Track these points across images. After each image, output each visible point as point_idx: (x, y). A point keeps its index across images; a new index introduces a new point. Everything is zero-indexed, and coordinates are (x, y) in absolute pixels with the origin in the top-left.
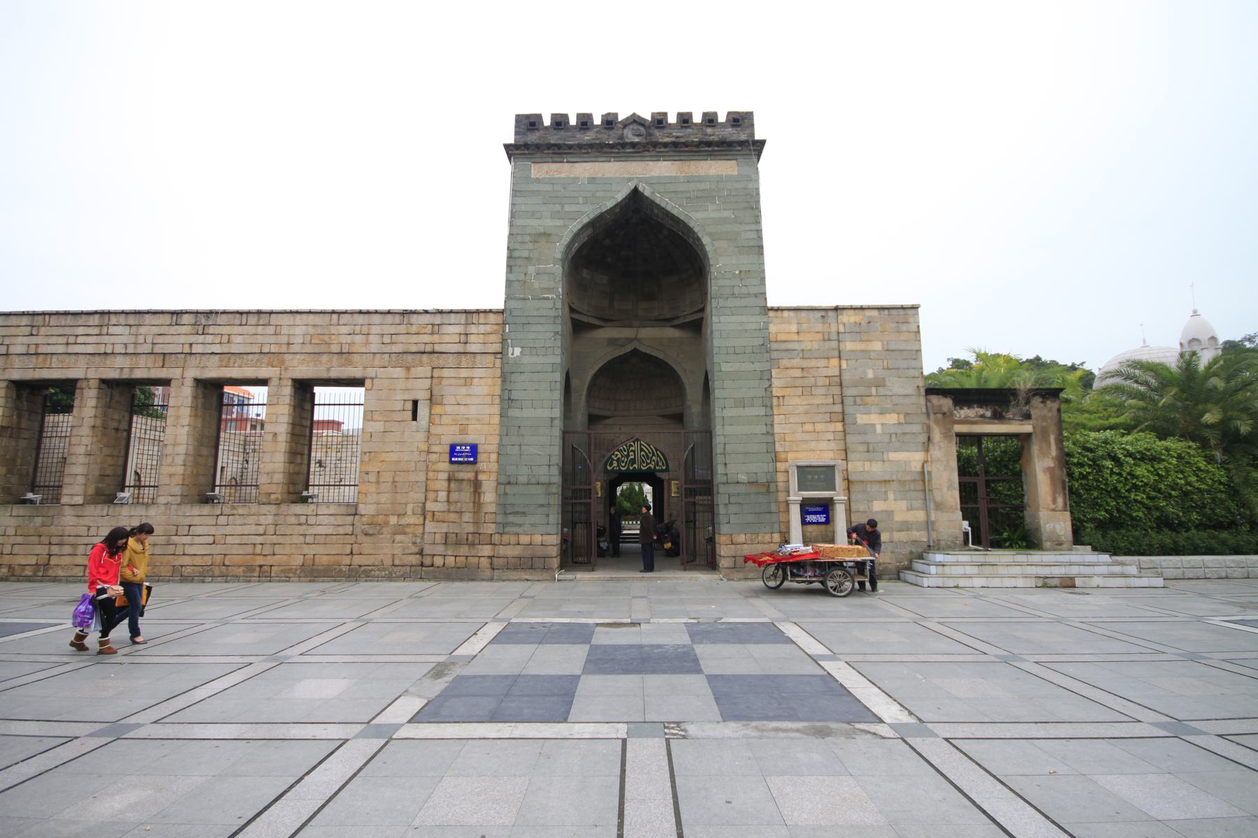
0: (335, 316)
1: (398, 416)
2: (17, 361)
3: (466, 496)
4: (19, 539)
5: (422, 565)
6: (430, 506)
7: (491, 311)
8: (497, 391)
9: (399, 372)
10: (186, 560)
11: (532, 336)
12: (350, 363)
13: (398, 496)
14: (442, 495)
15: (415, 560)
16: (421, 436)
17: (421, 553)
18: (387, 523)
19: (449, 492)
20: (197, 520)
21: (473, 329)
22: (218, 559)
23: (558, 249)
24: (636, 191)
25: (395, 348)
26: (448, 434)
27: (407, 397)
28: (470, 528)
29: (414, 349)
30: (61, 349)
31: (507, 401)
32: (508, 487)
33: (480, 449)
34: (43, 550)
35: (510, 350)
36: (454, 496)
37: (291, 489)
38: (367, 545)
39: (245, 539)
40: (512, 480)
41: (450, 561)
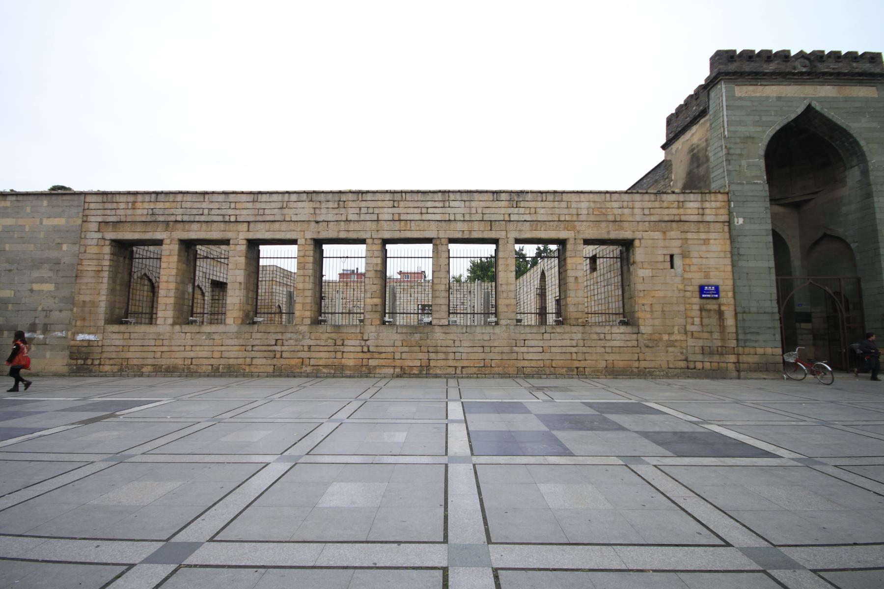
0: (608, 195)
1: (661, 266)
3: (714, 321)
4: (406, 349)
5: (688, 368)
6: (689, 328)
8: (728, 248)
9: (658, 235)
10: (526, 364)
11: (750, 210)
12: (622, 228)
13: (667, 321)
14: (697, 320)
15: (683, 364)
16: (678, 280)
17: (686, 360)
18: (661, 339)
19: (701, 318)
20: (529, 336)
21: (707, 205)
22: (548, 363)
23: (761, 147)
24: (809, 108)
25: (653, 218)
26: (698, 279)
27: (666, 252)
28: (719, 343)
29: (666, 218)
31: (735, 256)
32: (745, 316)
33: (721, 289)
34: (424, 356)
35: (736, 220)
36: (706, 321)
38: (648, 354)
39: (564, 349)
40: (747, 310)
41: (707, 365)
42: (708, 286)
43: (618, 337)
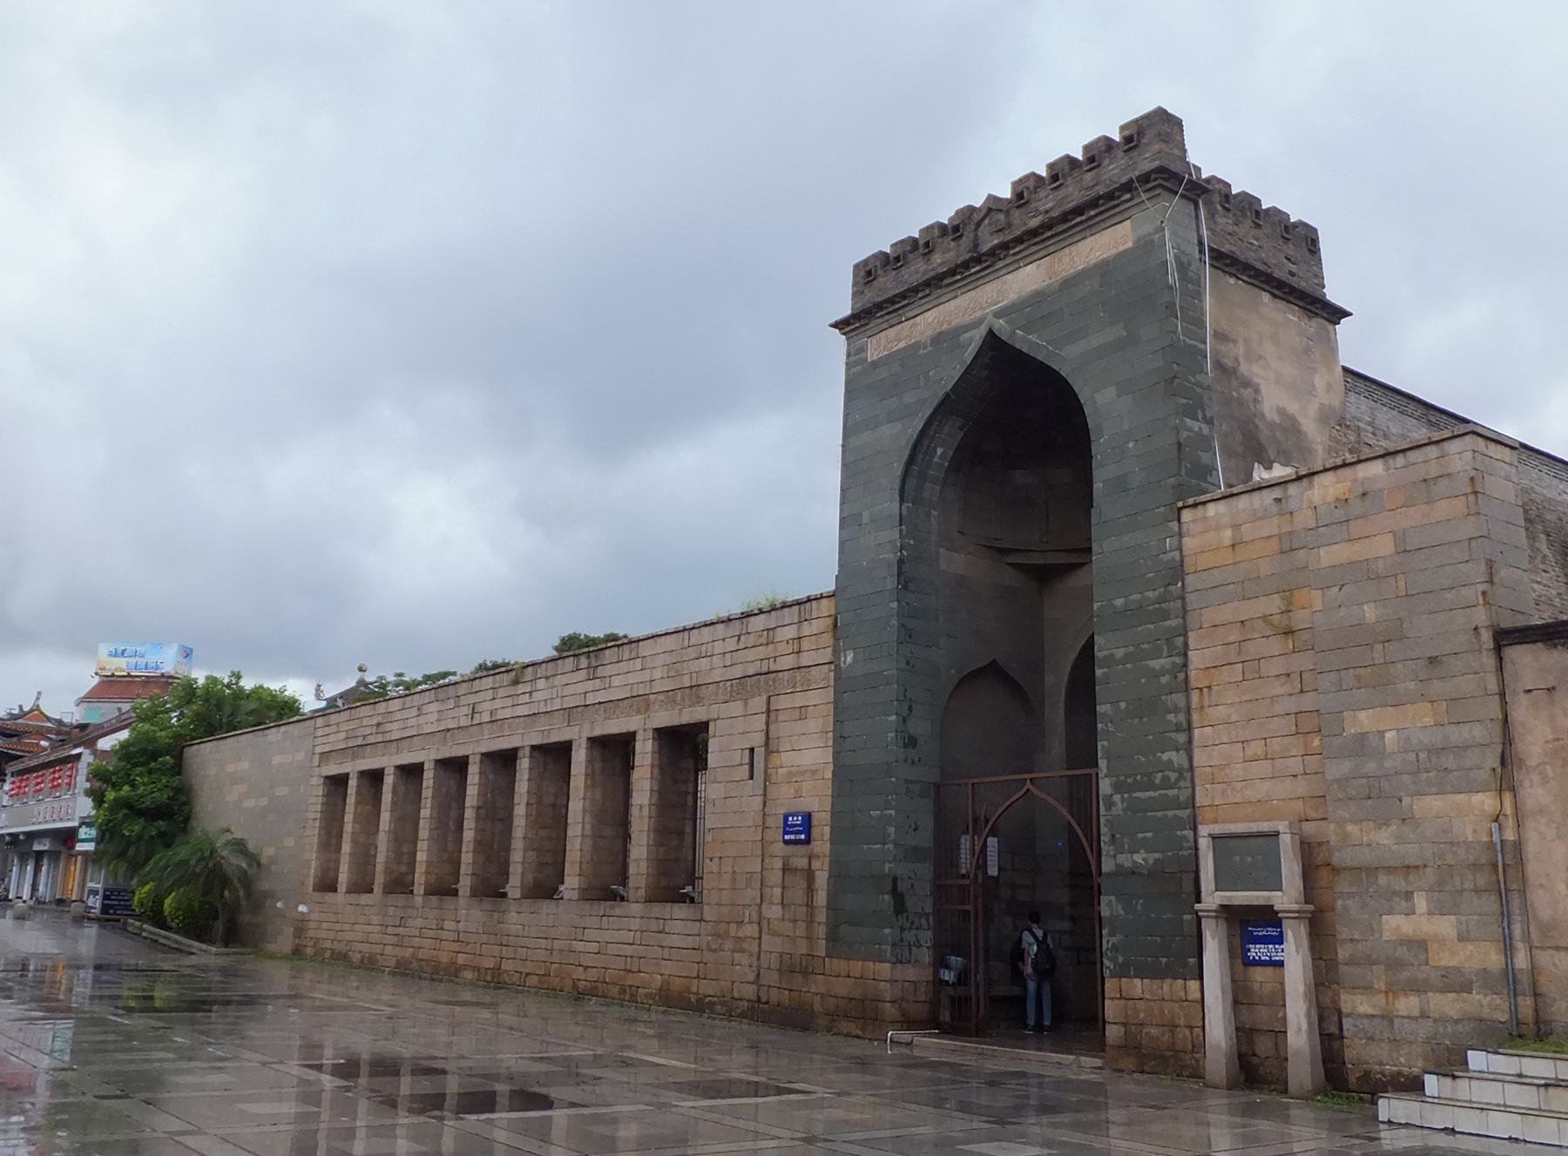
3: (797, 894)
5: (759, 1000)
7: (822, 597)
9: (736, 708)
10: (579, 973)
12: (698, 700)
21: (807, 629)
25: (737, 672)
26: (786, 800)
30: (508, 713)
33: (815, 822)
37: (663, 883)
43: (678, 926)
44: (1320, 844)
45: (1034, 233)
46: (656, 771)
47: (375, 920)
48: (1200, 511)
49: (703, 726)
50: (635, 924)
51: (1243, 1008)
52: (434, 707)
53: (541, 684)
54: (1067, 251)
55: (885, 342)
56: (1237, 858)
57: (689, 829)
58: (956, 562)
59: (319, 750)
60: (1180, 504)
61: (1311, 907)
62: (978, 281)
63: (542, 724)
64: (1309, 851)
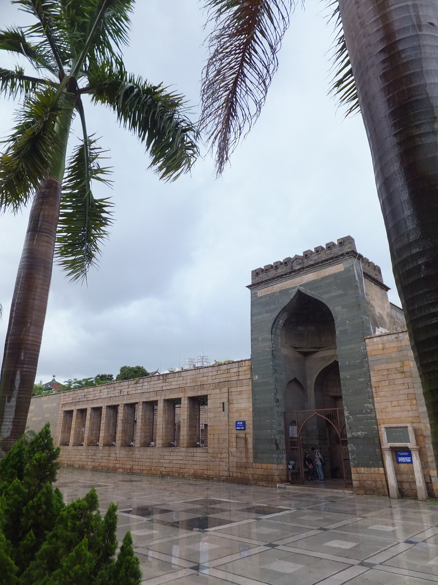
2: (126, 397)
4: (127, 459)
5: (229, 476)
6: (231, 450)
7: (246, 360)
9: (217, 391)
10: (163, 469)
12: (203, 389)
16: (226, 418)
21: (241, 369)
25: (217, 381)
26: (235, 417)
28: (244, 460)
29: (222, 380)
30: (134, 392)
33: (246, 424)
34: (131, 463)
37: (191, 442)
42: (239, 422)
43: (199, 455)
44: (419, 429)
45: (312, 265)
46: (189, 409)
47: (84, 454)
48: (371, 340)
49: (206, 396)
50: (183, 454)
51: (398, 476)
52: (106, 390)
53: (146, 384)
54: (322, 270)
55: (262, 292)
56: (394, 434)
57: (198, 425)
58: (285, 351)
59: (61, 403)
60: (365, 338)
61: (418, 447)
62: (294, 277)
63: (147, 395)
64: (415, 431)
